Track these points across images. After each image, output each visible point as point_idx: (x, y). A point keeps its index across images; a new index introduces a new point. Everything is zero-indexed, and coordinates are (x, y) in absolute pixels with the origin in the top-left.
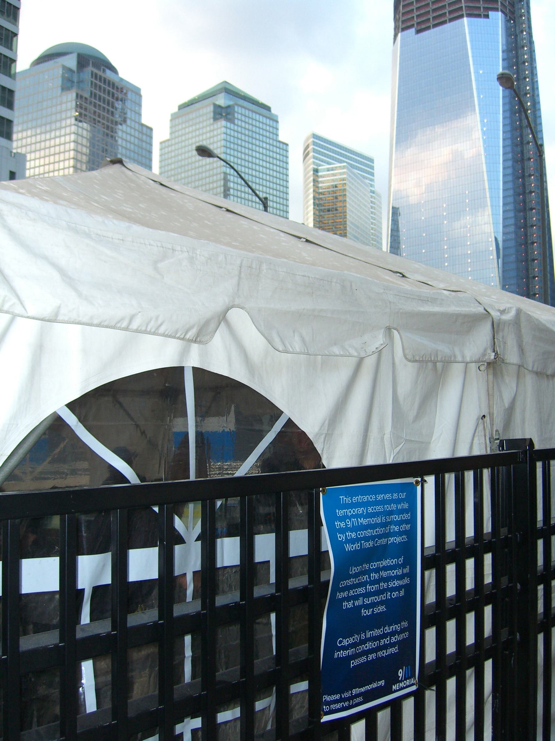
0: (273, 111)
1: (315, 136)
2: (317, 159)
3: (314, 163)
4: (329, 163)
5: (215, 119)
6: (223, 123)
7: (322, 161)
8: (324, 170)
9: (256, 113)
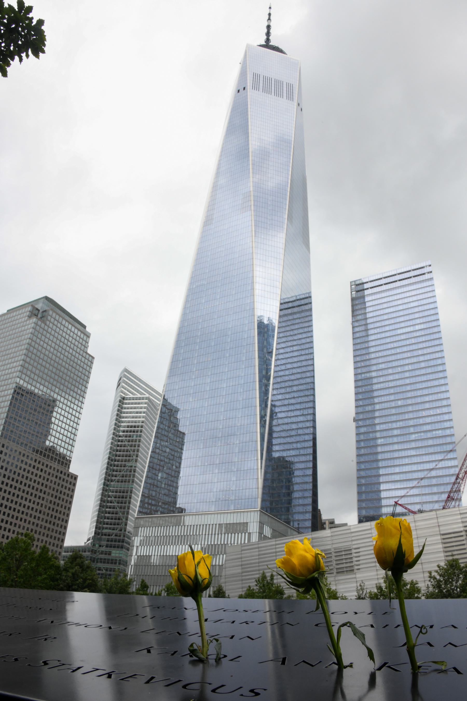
0: (87, 329)
1: (126, 370)
2: (125, 389)
5: (30, 317)
6: (34, 320)
7: (130, 392)
8: (130, 399)
9: (69, 323)
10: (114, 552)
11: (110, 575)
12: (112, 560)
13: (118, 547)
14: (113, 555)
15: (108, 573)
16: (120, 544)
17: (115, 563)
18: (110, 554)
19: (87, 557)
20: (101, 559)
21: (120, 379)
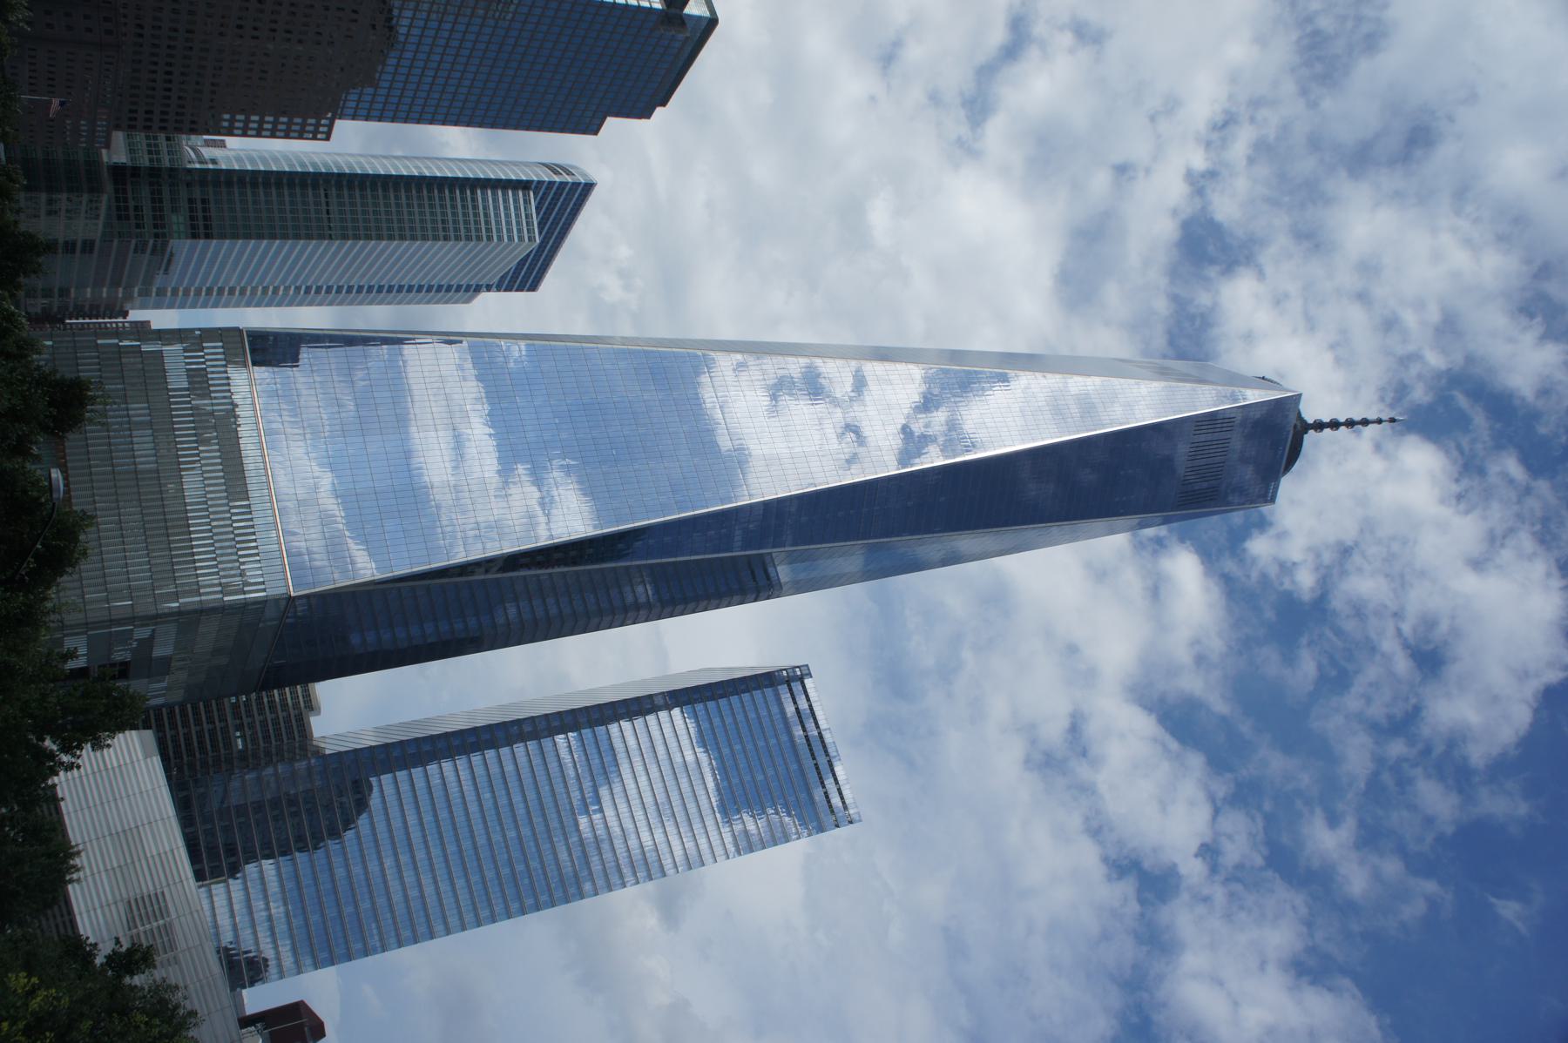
1: (589, 187)
3: (540, 183)
4: (538, 209)
8: (527, 202)
10: (181, 219)
11: (127, 217)
12: (162, 218)
13: (193, 227)
14: (174, 218)
15: (132, 213)
16: (202, 230)
17: (156, 226)
18: (174, 210)
19: (159, 160)
20: (160, 192)
21: (569, 173)
